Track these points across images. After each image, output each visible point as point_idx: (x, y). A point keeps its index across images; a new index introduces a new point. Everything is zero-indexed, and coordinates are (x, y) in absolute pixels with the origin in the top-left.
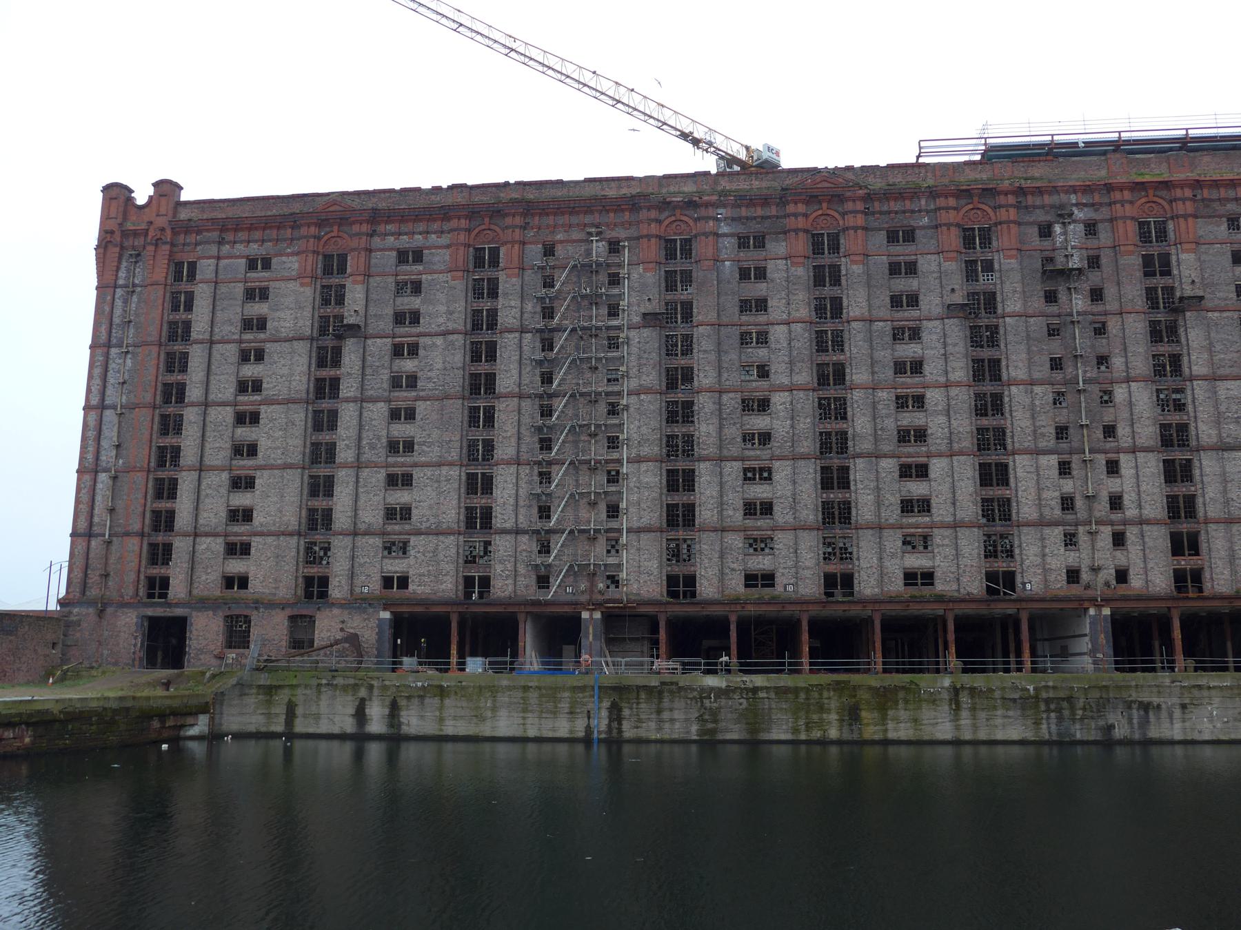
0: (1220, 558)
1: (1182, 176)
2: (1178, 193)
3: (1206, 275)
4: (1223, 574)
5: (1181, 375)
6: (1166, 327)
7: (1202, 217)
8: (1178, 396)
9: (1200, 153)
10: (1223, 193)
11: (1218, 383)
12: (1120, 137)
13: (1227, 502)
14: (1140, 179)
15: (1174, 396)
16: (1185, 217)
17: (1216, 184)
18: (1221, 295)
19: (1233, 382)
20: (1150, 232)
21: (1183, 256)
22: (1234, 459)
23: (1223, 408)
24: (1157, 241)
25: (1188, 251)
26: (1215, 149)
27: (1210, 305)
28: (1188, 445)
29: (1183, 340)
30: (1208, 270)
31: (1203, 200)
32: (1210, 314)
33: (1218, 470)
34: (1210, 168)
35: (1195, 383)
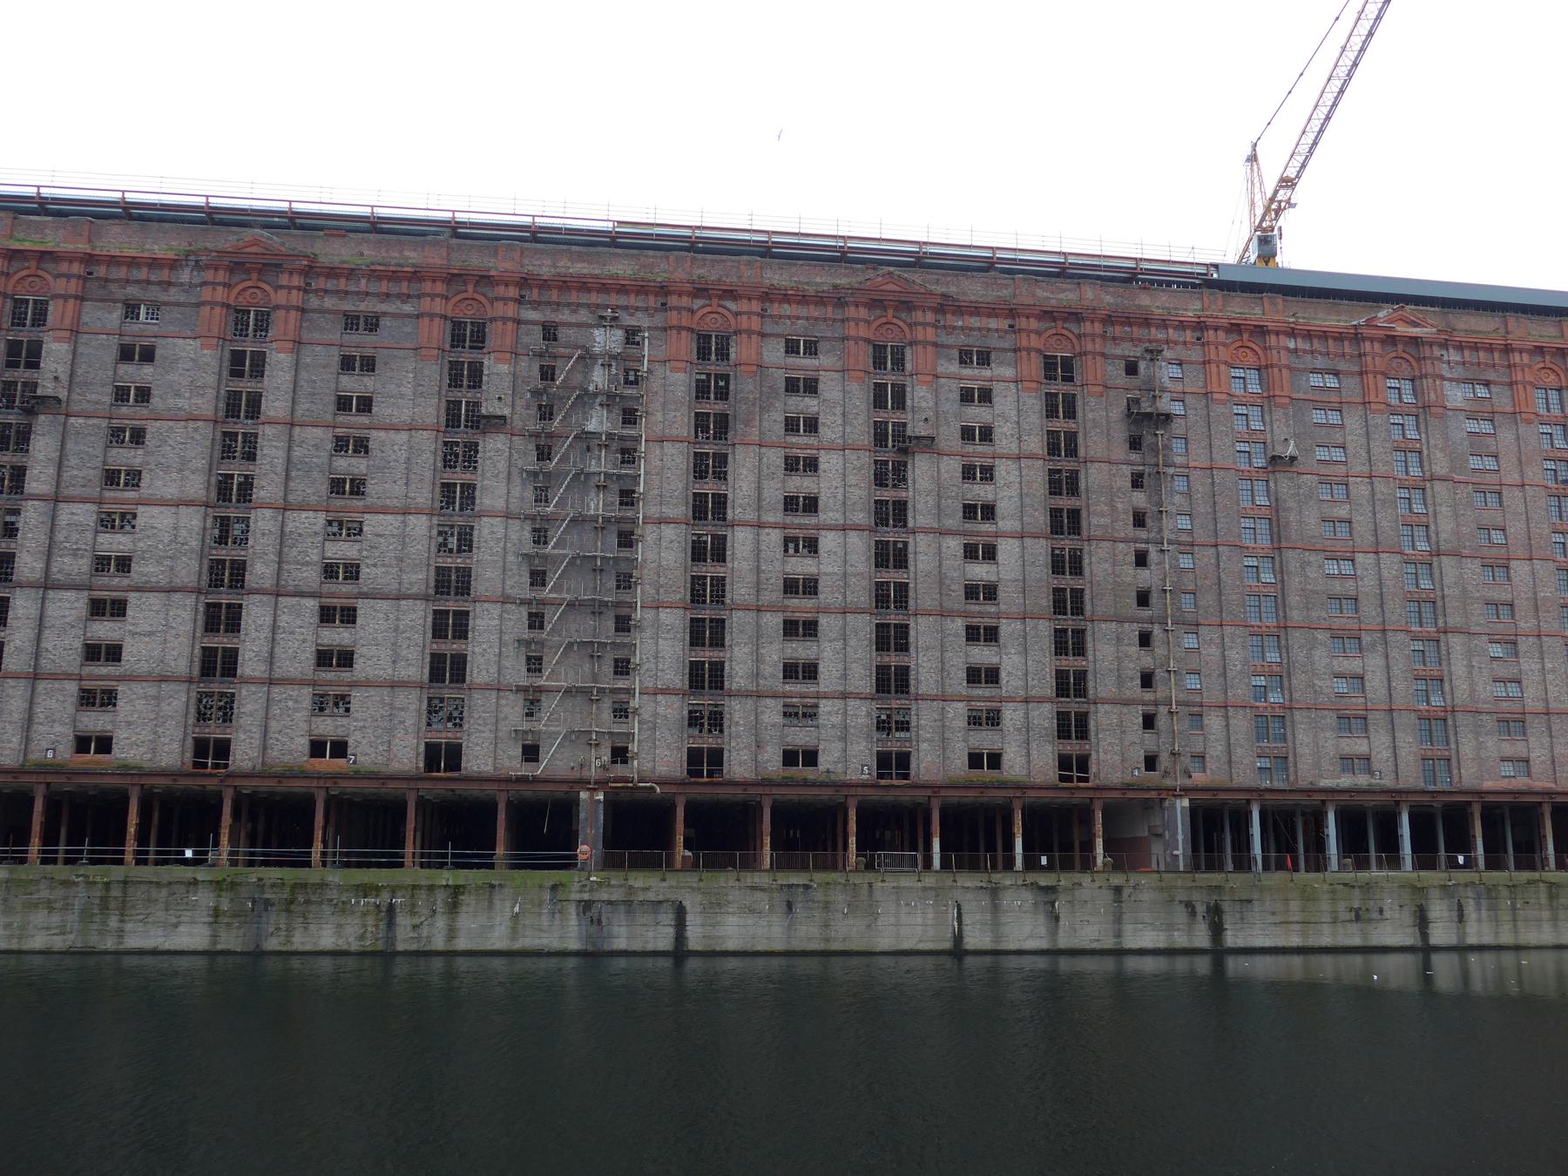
0: (10, 722)
1: (70, 247)
2: (64, 267)
3: (80, 372)
4: (10, 742)
5: (1079, 534)
6: (18, 432)
7: (91, 300)
8: (13, 519)
9: (111, 221)
10: (122, 273)
11: (62, 505)
12: (39, 193)
13: (37, 655)
14: (16, 246)
15: (8, 518)
16: (65, 297)
17: (113, 261)
18: (93, 397)
19: (81, 505)
20: (26, 313)
21: (55, 346)
22: (60, 600)
23: (60, 537)
24: (33, 325)
25: (59, 340)
26: (174, 220)
27: (74, 408)
28: (11, 580)
29: (31, 448)
30: (84, 366)
31: (98, 278)
32: (72, 420)
33: (34, 612)
34: (116, 241)
35: (30, 503)
